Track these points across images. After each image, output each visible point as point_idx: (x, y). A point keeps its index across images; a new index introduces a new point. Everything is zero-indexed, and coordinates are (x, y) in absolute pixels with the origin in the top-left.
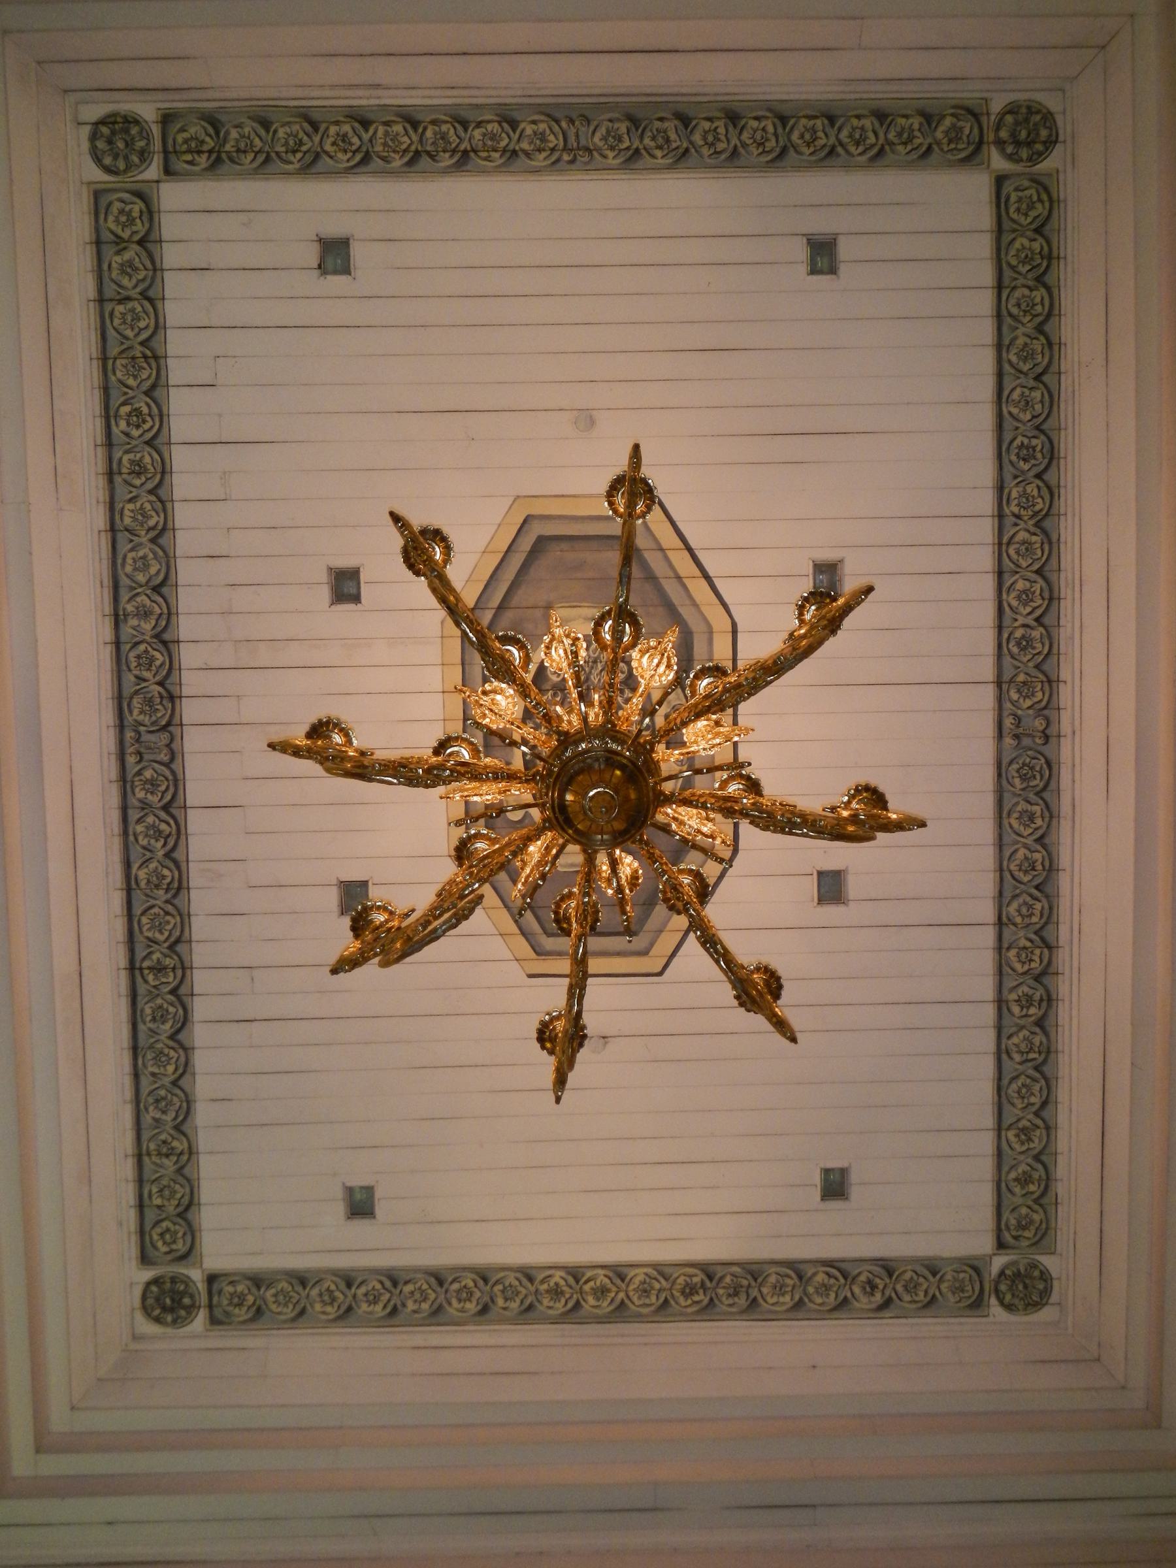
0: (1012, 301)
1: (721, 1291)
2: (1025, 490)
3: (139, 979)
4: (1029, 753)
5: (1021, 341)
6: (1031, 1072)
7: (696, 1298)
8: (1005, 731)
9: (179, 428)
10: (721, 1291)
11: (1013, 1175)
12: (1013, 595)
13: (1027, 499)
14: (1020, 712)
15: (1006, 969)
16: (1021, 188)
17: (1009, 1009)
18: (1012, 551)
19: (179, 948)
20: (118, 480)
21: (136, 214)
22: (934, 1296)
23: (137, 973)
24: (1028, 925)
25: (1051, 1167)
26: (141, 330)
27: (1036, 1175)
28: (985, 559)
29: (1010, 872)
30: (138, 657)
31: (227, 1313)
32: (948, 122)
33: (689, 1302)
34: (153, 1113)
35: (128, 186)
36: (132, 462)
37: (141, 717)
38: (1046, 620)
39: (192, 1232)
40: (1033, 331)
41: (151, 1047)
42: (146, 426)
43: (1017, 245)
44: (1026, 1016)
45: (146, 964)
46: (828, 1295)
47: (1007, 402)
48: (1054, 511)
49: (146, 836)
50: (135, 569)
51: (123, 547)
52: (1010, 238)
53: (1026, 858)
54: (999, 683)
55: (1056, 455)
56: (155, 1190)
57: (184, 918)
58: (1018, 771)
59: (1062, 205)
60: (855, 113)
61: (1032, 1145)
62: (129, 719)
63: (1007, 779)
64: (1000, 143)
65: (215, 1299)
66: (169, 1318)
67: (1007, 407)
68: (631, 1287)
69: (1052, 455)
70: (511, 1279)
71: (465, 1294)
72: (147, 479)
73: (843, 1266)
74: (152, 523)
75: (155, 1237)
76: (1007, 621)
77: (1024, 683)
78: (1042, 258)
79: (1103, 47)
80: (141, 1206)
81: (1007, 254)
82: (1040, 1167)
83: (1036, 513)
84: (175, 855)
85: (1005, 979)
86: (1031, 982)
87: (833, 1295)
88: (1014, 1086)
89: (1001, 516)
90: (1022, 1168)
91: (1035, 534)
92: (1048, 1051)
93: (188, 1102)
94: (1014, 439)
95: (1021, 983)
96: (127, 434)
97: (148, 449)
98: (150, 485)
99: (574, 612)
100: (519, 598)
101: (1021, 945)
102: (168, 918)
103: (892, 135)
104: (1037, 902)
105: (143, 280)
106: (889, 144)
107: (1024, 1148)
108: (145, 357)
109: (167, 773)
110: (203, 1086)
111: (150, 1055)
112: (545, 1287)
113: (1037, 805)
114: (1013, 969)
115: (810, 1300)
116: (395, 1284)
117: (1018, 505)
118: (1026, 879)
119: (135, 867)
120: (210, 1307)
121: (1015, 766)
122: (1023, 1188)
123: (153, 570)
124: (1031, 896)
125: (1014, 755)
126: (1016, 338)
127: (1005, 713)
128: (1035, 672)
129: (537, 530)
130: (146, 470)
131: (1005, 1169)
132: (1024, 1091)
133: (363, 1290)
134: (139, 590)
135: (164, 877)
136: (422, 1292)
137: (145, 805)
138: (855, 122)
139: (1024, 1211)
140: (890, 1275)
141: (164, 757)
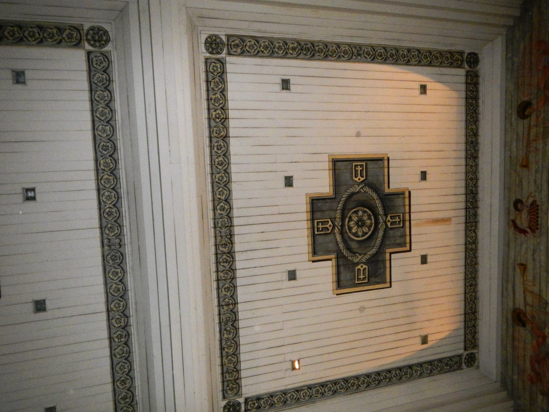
0: (96, 96)
2: (106, 161)
4: (114, 251)
5: (101, 109)
8: (105, 244)
11: (120, 397)
12: (104, 197)
13: (107, 164)
14: (110, 238)
15: (112, 327)
16: (97, 56)
17: (114, 341)
24: (118, 311)
25: (134, 392)
27: (129, 396)
32: (68, 31)
38: (117, 205)
40: (105, 106)
43: (97, 76)
44: (120, 342)
48: (117, 167)
52: (94, 73)
53: (116, 287)
54: (101, 228)
58: (111, 258)
59: (113, 63)
60: (30, 26)
61: (126, 386)
63: (107, 261)
64: (88, 41)
67: (97, 132)
69: (115, 149)
76: (102, 206)
77: (111, 227)
78: (107, 81)
79: (121, 11)
81: (93, 78)
82: (130, 392)
83: (111, 169)
86: (121, 330)
88: (118, 366)
89: (97, 170)
90: (124, 394)
92: (129, 352)
95: (117, 331)
103: (45, 35)
104: (121, 302)
106: (45, 38)
107: (124, 387)
113: (119, 269)
117: (104, 166)
121: (109, 256)
124: (119, 300)
125: (109, 252)
126: (98, 108)
127: (104, 238)
131: (117, 395)
138: (30, 29)
139: (125, 408)
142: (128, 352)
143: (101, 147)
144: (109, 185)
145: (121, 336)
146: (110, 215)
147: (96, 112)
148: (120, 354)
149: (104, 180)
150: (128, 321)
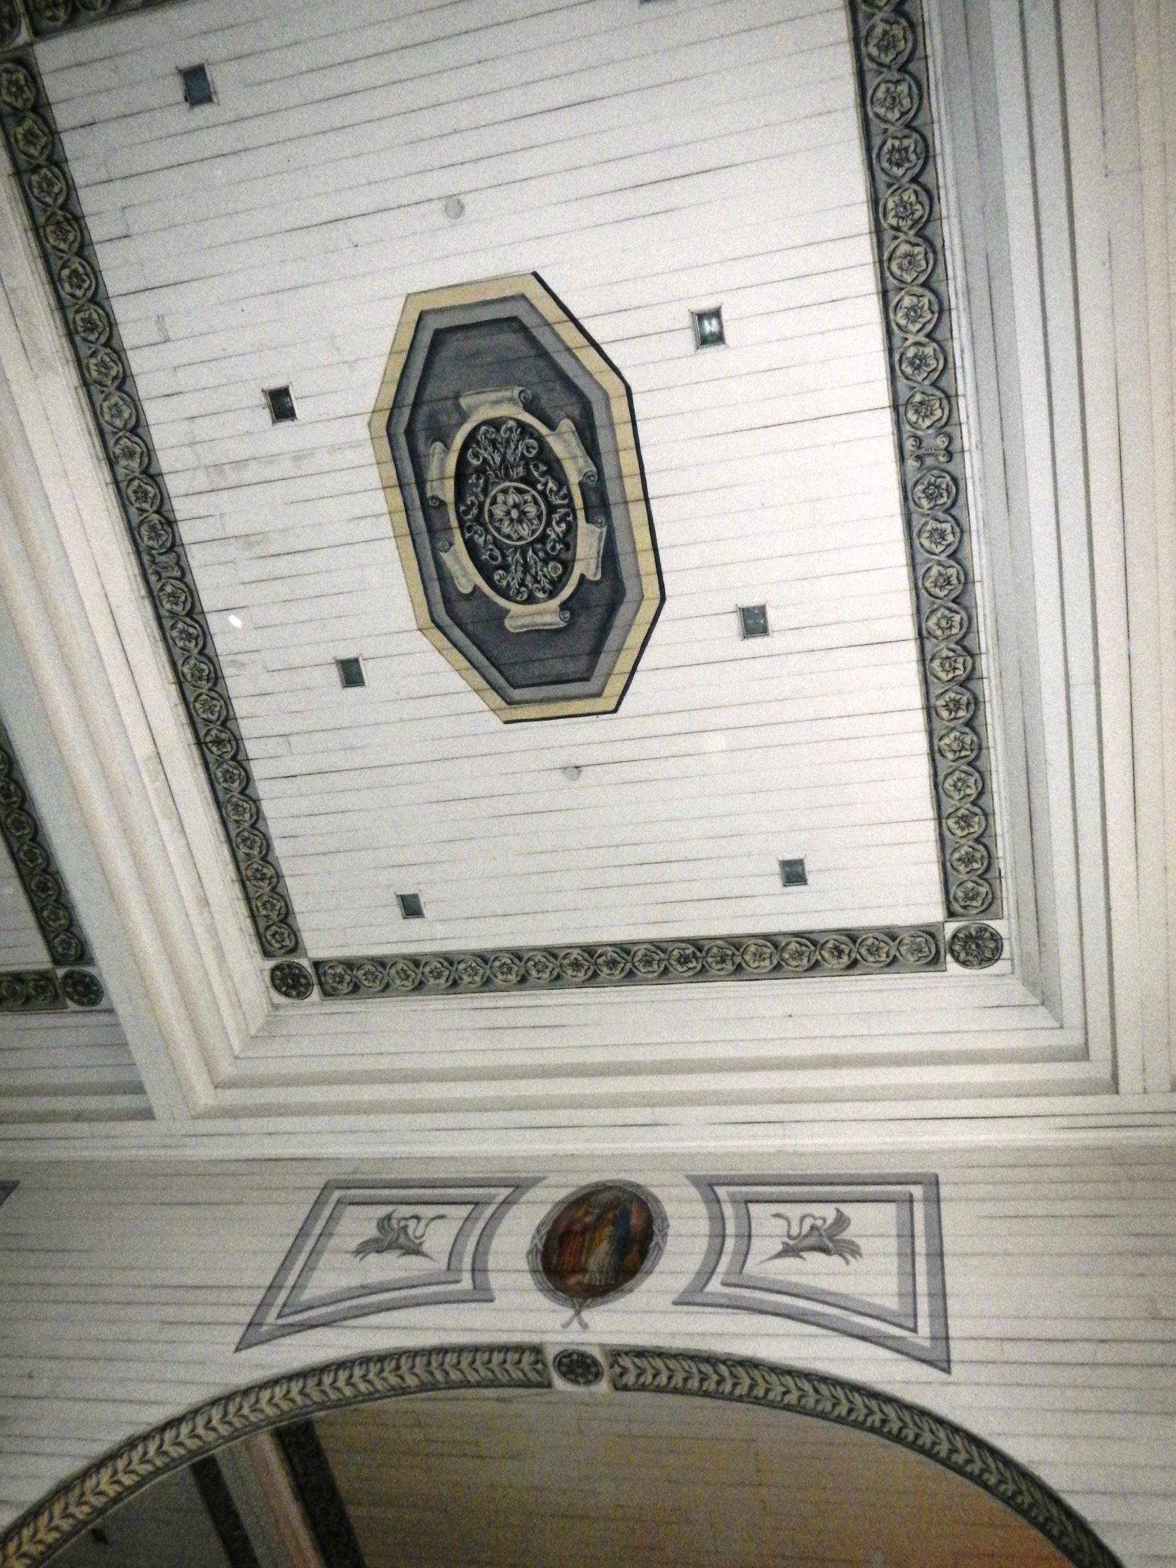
1: (710, 960)
2: (901, 199)
3: (207, 752)
4: (935, 472)
5: (879, 30)
6: (965, 768)
7: (690, 965)
8: (907, 454)
9: (113, 282)
10: (710, 960)
11: (957, 855)
12: (900, 314)
13: (905, 208)
14: (920, 433)
15: (931, 679)
17: (938, 715)
18: (894, 268)
19: (229, 724)
20: (77, 339)
21: (22, 82)
22: (895, 957)
23: (204, 746)
25: (992, 849)
26: (57, 194)
27: (978, 855)
28: (867, 280)
29: (926, 589)
30: (135, 492)
31: (335, 989)
33: (685, 968)
34: (242, 850)
35: (8, 55)
36: (83, 320)
37: (151, 543)
38: (938, 335)
39: (294, 933)
41: (229, 801)
42: (86, 285)
44: (955, 718)
45: (208, 739)
46: (801, 959)
47: (872, 103)
48: (935, 215)
49: (181, 639)
50: (112, 416)
51: (98, 398)
53: (940, 574)
54: (895, 407)
55: (931, 154)
56: (260, 904)
57: (227, 702)
58: (924, 491)
61: (972, 830)
62: (142, 547)
65: (323, 979)
66: (294, 993)
68: (636, 959)
69: (927, 155)
70: (539, 957)
71: (507, 969)
72: (100, 334)
73: (812, 936)
74: (113, 373)
75: (269, 938)
76: (897, 342)
77: (922, 403)
80: (253, 917)
82: (981, 848)
83: (916, 222)
84: (207, 651)
85: (932, 688)
86: (958, 689)
87: (806, 960)
88: (950, 781)
89: (878, 231)
91: (918, 245)
92: (980, 748)
93: (267, 840)
94: (884, 143)
96: (73, 296)
97: (92, 306)
98: (103, 339)
99: (482, 397)
100: (431, 390)
101: (944, 655)
102: (215, 702)
105: (45, 147)
108: (67, 220)
109: (183, 586)
110: (275, 827)
111: (230, 807)
112: (567, 961)
114: (938, 679)
115: (787, 964)
116: (451, 964)
117: (896, 216)
118: (942, 594)
119: (179, 667)
120: (321, 984)
121: (920, 487)
122: (966, 866)
123: (126, 415)
124: (949, 609)
126: (873, 28)
127: (905, 436)
128: (930, 390)
129: (433, 324)
130: (97, 326)
131: (948, 851)
132: (960, 784)
133: (427, 969)
134: (120, 434)
135: (203, 670)
136: (473, 969)
137: (173, 615)
139: (970, 885)
140: (854, 942)
141: (178, 574)
142: (976, 746)
143: (885, 157)
144: (915, 275)
145: (957, 702)
146: (918, 368)
147: (867, 44)
148: (955, 752)
149: (899, 260)
150: (974, 668)
